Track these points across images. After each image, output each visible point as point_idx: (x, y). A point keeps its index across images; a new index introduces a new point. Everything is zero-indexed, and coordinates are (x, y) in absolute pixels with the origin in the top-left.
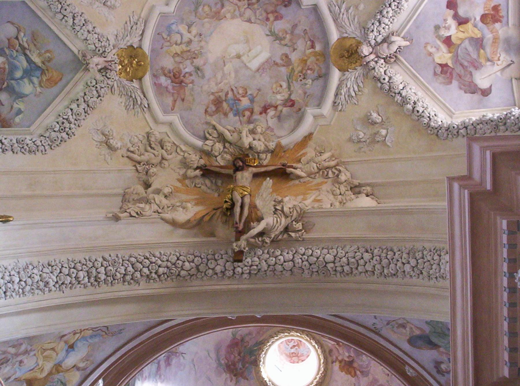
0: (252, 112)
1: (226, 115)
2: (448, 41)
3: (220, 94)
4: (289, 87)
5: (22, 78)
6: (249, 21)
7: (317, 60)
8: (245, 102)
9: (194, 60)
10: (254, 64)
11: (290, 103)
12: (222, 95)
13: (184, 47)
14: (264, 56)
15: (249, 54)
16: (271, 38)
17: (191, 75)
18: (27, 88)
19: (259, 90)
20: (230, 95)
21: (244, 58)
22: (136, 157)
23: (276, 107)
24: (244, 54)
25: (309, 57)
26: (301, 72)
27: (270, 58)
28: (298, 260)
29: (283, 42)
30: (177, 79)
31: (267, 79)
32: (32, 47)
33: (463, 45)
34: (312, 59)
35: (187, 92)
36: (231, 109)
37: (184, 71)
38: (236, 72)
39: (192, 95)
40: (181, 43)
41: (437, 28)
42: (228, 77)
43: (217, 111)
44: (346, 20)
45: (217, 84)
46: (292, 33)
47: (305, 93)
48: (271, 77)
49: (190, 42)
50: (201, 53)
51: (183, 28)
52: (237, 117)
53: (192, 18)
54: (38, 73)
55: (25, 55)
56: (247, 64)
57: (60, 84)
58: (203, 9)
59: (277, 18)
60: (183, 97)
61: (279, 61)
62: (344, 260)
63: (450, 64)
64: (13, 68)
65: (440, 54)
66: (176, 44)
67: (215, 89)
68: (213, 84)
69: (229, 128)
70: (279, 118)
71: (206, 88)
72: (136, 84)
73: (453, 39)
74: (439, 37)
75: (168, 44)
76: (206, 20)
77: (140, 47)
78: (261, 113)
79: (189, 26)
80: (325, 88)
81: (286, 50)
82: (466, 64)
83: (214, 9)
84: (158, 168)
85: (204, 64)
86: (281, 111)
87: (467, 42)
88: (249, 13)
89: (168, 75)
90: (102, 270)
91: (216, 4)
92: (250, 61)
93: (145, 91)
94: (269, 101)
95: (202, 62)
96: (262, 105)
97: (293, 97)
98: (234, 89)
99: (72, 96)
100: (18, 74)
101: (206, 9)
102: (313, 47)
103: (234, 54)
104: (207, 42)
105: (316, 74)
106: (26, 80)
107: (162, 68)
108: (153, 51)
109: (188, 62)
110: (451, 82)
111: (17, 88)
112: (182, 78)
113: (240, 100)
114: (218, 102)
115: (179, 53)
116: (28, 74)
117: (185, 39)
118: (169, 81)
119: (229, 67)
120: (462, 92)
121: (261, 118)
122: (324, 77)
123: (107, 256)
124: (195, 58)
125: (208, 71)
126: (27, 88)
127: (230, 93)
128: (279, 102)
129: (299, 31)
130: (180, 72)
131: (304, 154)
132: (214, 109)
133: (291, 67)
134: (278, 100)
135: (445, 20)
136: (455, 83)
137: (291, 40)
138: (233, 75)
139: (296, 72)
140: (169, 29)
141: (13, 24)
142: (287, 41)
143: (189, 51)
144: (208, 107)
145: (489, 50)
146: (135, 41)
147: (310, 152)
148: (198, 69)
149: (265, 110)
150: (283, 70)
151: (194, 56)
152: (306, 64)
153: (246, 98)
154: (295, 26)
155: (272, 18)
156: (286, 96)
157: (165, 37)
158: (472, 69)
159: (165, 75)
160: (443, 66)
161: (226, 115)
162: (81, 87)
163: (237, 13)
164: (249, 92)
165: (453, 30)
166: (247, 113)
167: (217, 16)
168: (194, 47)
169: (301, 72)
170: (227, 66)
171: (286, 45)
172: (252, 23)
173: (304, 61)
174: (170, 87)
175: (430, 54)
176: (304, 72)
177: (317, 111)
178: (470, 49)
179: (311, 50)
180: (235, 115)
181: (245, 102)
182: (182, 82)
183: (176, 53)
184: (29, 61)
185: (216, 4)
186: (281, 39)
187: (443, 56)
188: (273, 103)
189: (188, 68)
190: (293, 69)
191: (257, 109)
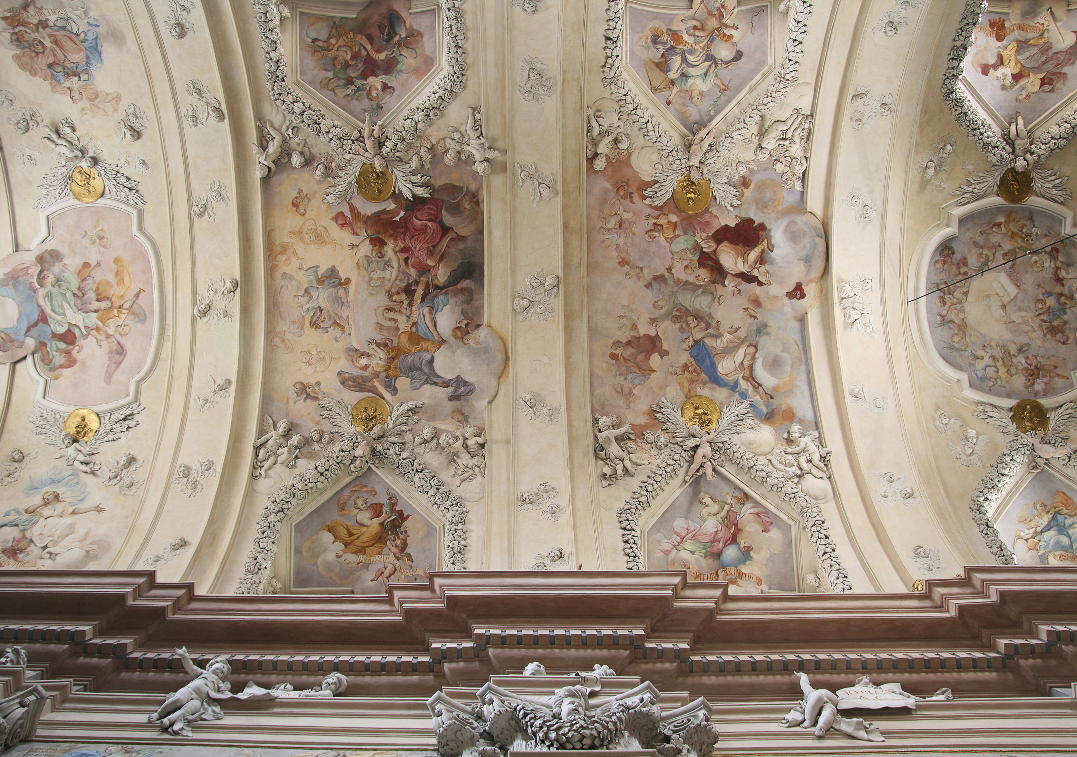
1: (1065, 323)
3: (1044, 328)
6: (966, 294)
7: (1014, 220)
8: (1051, 301)
9: (1012, 353)
10: (1012, 290)
11: (1054, 253)
12: (1045, 325)
15: (1001, 295)
19: (1039, 285)
21: (1006, 300)
23: (1057, 268)
24: (1001, 301)
25: (1010, 229)
26: (1023, 239)
27: (1006, 272)
29: (991, 258)
31: (1028, 276)
34: (1011, 226)
35: (1047, 362)
36: (1059, 317)
38: (1020, 309)
39: (1049, 357)
40: (996, 367)
42: (1026, 319)
43: (1063, 332)
44: (982, 185)
45: (1035, 331)
46: (982, 247)
47: (1046, 235)
48: (1026, 273)
50: (1003, 346)
52: (1067, 310)
53: (967, 354)
56: (1012, 297)
58: (957, 343)
59: (965, 264)
60: (1052, 367)
66: (997, 372)
67: (1039, 333)
68: (1034, 335)
70: (1068, 265)
71: (1039, 343)
75: (998, 380)
76: (968, 339)
78: (1063, 285)
80: (1044, 214)
81: (999, 255)
83: (956, 331)
85: (1015, 343)
86: (1062, 262)
88: (958, 294)
89: (1031, 381)
91: (950, 328)
92: (1010, 295)
93: (1057, 405)
94: (1051, 276)
95: (1013, 345)
96: (1055, 283)
98: (1037, 313)
101: (956, 339)
102: (999, 225)
104: (992, 340)
105: (1028, 223)
108: (1009, 396)
109: (1014, 360)
112: (1032, 367)
113: (1049, 307)
114: (1053, 331)
115: (1006, 369)
117: (991, 362)
118: (1038, 381)
119: (1015, 317)
121: (1067, 284)
122: (1031, 215)
124: (1009, 353)
125: (1023, 340)
127: (1042, 317)
128: (1053, 265)
129: (980, 240)
132: (1060, 335)
133: (1017, 250)
134: (1050, 266)
138: (1023, 314)
139: (1023, 244)
141: (1014, 543)
142: (990, 254)
143: (1003, 359)
144: (1060, 342)
148: (1021, 350)
149: (1059, 280)
151: (1007, 354)
152: (1016, 233)
153: (1047, 300)
154: (975, 244)
155: (964, 269)
156: (1047, 256)
157: (991, 384)
163: (958, 306)
164: (1041, 297)
166: (1063, 299)
167: (963, 327)
168: (998, 353)
169: (1023, 239)
170: (1015, 320)
171: (994, 255)
172: (968, 291)
173: (1013, 236)
176: (1023, 236)
179: (1003, 227)
180: (1065, 313)
181: (1051, 301)
182: (1036, 367)
183: (1007, 372)
185: (950, 328)
188: (1053, 271)
189: (1021, 361)
190: (1019, 248)
191: (1058, 289)
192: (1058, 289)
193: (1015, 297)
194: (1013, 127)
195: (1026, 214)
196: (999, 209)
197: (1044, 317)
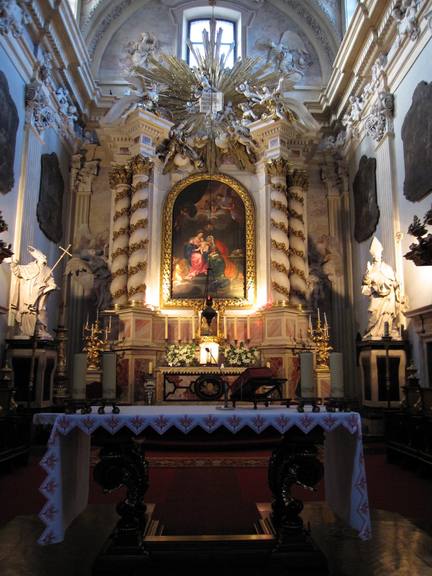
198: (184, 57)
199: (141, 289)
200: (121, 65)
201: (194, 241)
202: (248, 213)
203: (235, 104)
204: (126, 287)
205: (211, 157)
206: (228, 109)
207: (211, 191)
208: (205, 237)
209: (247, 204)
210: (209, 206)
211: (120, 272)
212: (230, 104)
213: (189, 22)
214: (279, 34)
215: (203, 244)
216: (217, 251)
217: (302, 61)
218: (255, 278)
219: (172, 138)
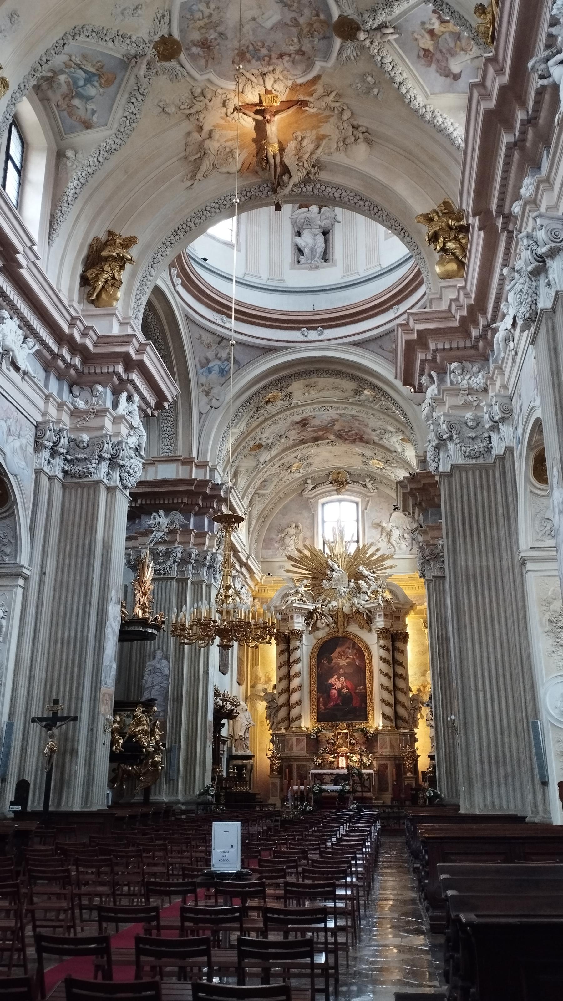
0: (270, 58)
1: (249, 61)
2: (432, 32)
4: (299, 41)
5: (85, 85)
8: (264, 51)
10: (269, 24)
13: (206, 20)
14: (276, 18)
16: (281, 5)
17: (216, 39)
18: (91, 91)
20: (251, 47)
22: (188, 112)
23: (290, 55)
28: (316, 192)
30: (205, 45)
31: (281, 35)
32: (85, 62)
33: (443, 36)
37: (209, 39)
38: (254, 31)
41: (423, 23)
49: (210, 15)
50: (222, 22)
51: (202, 7)
54: (96, 78)
55: (81, 68)
57: (117, 82)
61: (289, 22)
62: (346, 199)
63: (431, 49)
64: (75, 80)
65: (424, 41)
69: (255, 72)
70: (293, 62)
71: (230, 46)
72: (173, 63)
73: (436, 31)
74: (425, 29)
77: (170, 35)
79: (207, 4)
81: (294, 15)
82: (444, 51)
84: (205, 112)
87: (447, 34)
90: (193, 225)
97: (303, 49)
99: (128, 89)
100: (81, 83)
102: (318, 15)
103: (250, 18)
105: (321, 35)
106: (89, 86)
107: (192, 41)
108: (181, 31)
110: (430, 65)
111: (85, 93)
116: (88, 81)
119: (247, 28)
120: (438, 75)
123: (193, 215)
125: (230, 34)
126: (91, 91)
130: (206, 40)
131: (315, 90)
135: (430, 20)
136: (434, 66)
137: (298, 8)
138: (251, 32)
140: (190, 10)
145: (464, 42)
146: (164, 32)
147: (320, 89)
149: (281, 56)
150: (294, 29)
158: (448, 56)
159: (195, 45)
160: (426, 51)
161: (249, 61)
162: (133, 80)
165: (436, 25)
166: (267, 59)
168: (215, 18)
173: (310, 25)
174: (201, 53)
175: (416, 40)
177: (324, 64)
178: (449, 40)
181: (264, 51)
184: (85, 71)
186: (290, 6)
187: (427, 42)
188: (287, 52)
189: (212, 35)
191: (274, 56)
192: (274, 56)
193: (263, 27)
194: (391, 30)
195: (328, 35)
196: (330, 15)
197: (251, 47)
198: (321, 547)
199: (299, 718)
200: (276, 545)
201: (332, 681)
202: (367, 661)
203: (357, 580)
204: (289, 714)
205: (340, 622)
206: (352, 584)
207: (342, 645)
208: (338, 678)
209: (366, 655)
210: (341, 656)
211: (284, 705)
212: (353, 580)
213: (323, 504)
214: (388, 515)
215: (338, 683)
216: (347, 688)
217: (406, 535)
218: (372, 707)
219: (315, 610)
